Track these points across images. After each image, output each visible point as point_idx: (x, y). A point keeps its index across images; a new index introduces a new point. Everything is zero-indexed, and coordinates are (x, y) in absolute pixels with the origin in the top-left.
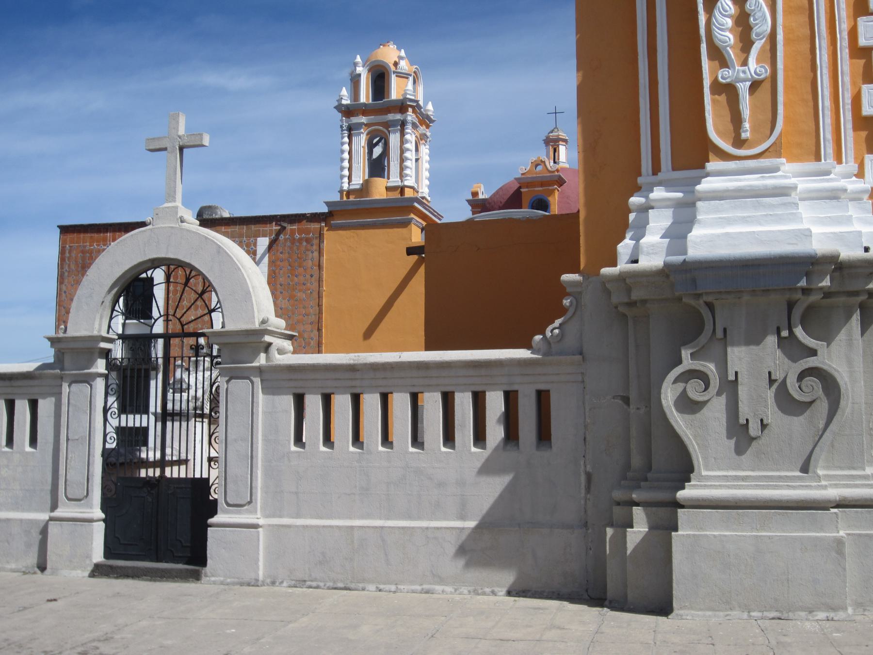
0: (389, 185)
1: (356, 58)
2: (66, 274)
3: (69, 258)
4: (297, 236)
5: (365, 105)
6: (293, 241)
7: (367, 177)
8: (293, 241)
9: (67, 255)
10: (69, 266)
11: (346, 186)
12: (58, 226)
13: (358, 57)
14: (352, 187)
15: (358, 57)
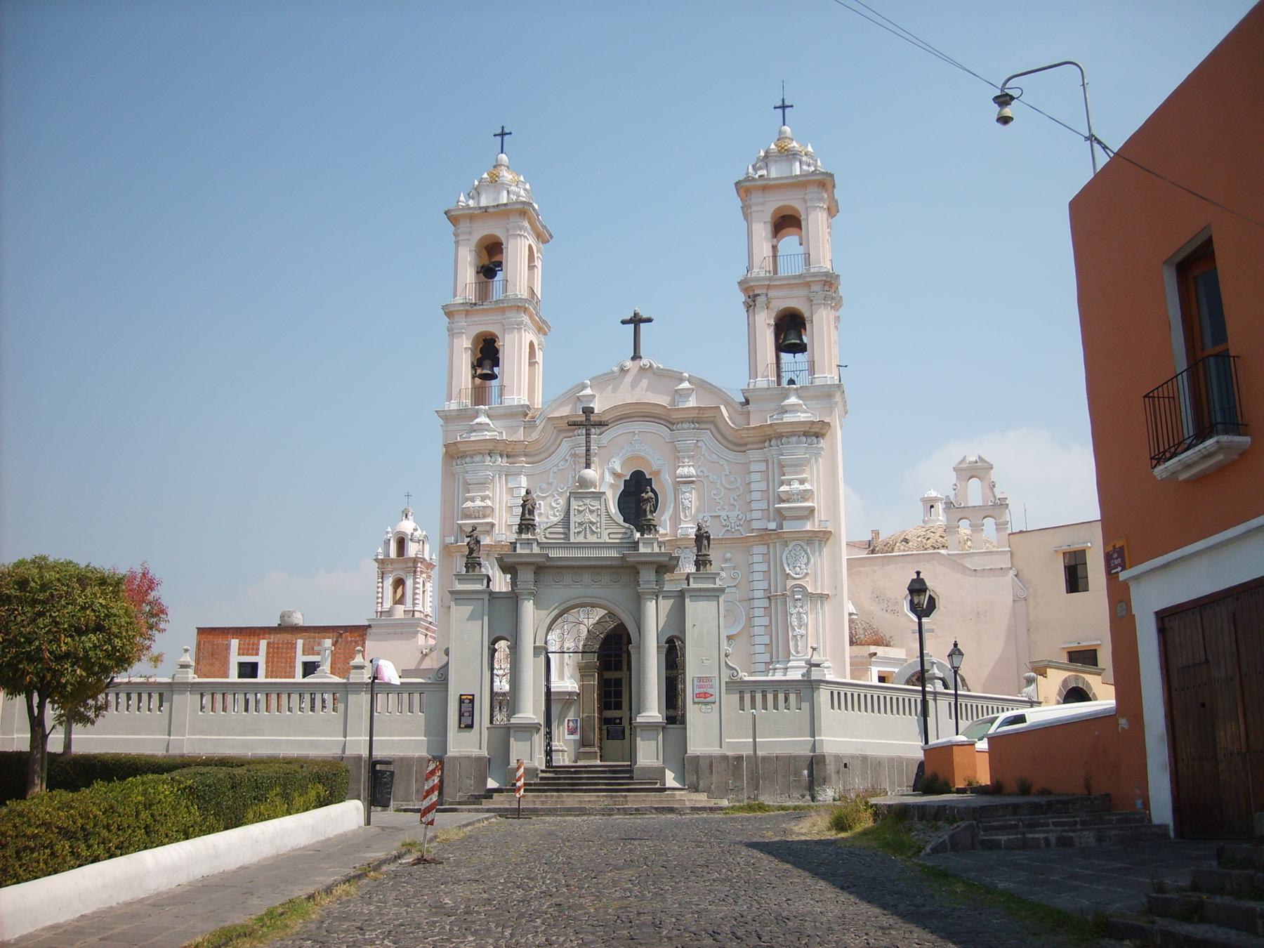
0: (406, 609)
1: (387, 528)
2: (201, 658)
3: (203, 648)
4: (349, 639)
5: (392, 559)
6: (347, 642)
7: (392, 604)
8: (347, 642)
9: (202, 646)
10: (203, 654)
11: (379, 609)
12: (197, 628)
13: (389, 528)
14: (383, 610)
15: (389, 528)
